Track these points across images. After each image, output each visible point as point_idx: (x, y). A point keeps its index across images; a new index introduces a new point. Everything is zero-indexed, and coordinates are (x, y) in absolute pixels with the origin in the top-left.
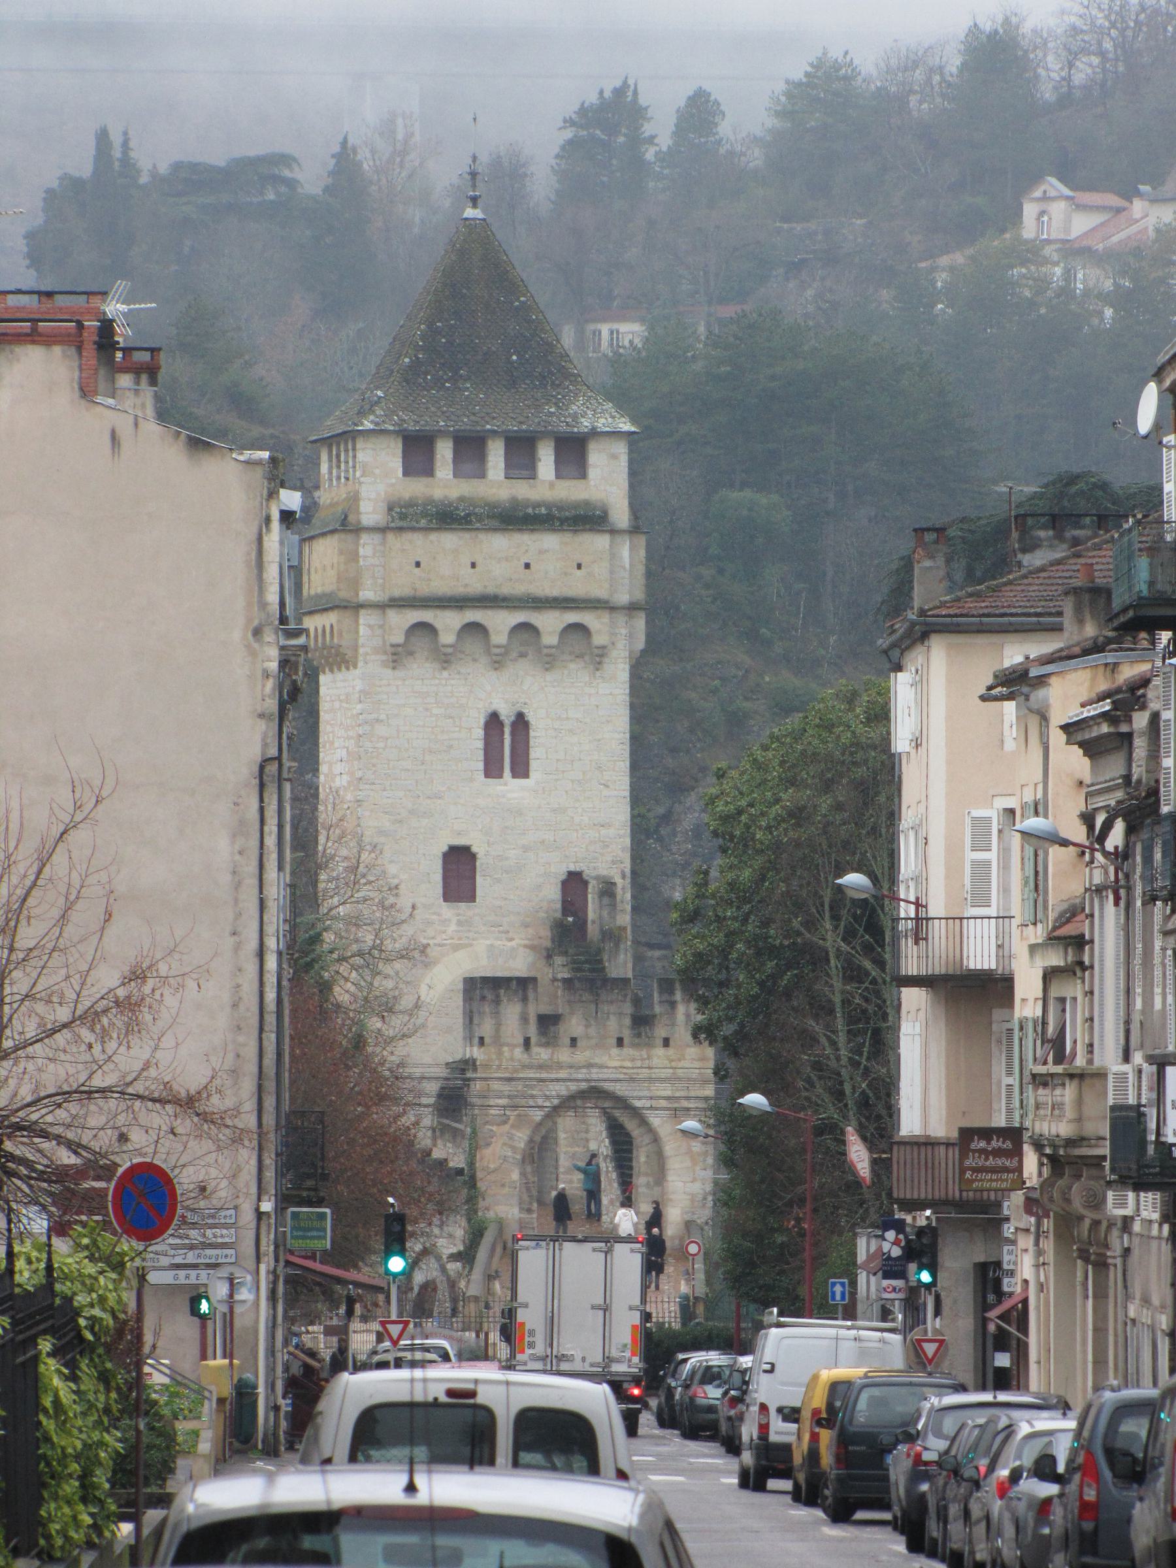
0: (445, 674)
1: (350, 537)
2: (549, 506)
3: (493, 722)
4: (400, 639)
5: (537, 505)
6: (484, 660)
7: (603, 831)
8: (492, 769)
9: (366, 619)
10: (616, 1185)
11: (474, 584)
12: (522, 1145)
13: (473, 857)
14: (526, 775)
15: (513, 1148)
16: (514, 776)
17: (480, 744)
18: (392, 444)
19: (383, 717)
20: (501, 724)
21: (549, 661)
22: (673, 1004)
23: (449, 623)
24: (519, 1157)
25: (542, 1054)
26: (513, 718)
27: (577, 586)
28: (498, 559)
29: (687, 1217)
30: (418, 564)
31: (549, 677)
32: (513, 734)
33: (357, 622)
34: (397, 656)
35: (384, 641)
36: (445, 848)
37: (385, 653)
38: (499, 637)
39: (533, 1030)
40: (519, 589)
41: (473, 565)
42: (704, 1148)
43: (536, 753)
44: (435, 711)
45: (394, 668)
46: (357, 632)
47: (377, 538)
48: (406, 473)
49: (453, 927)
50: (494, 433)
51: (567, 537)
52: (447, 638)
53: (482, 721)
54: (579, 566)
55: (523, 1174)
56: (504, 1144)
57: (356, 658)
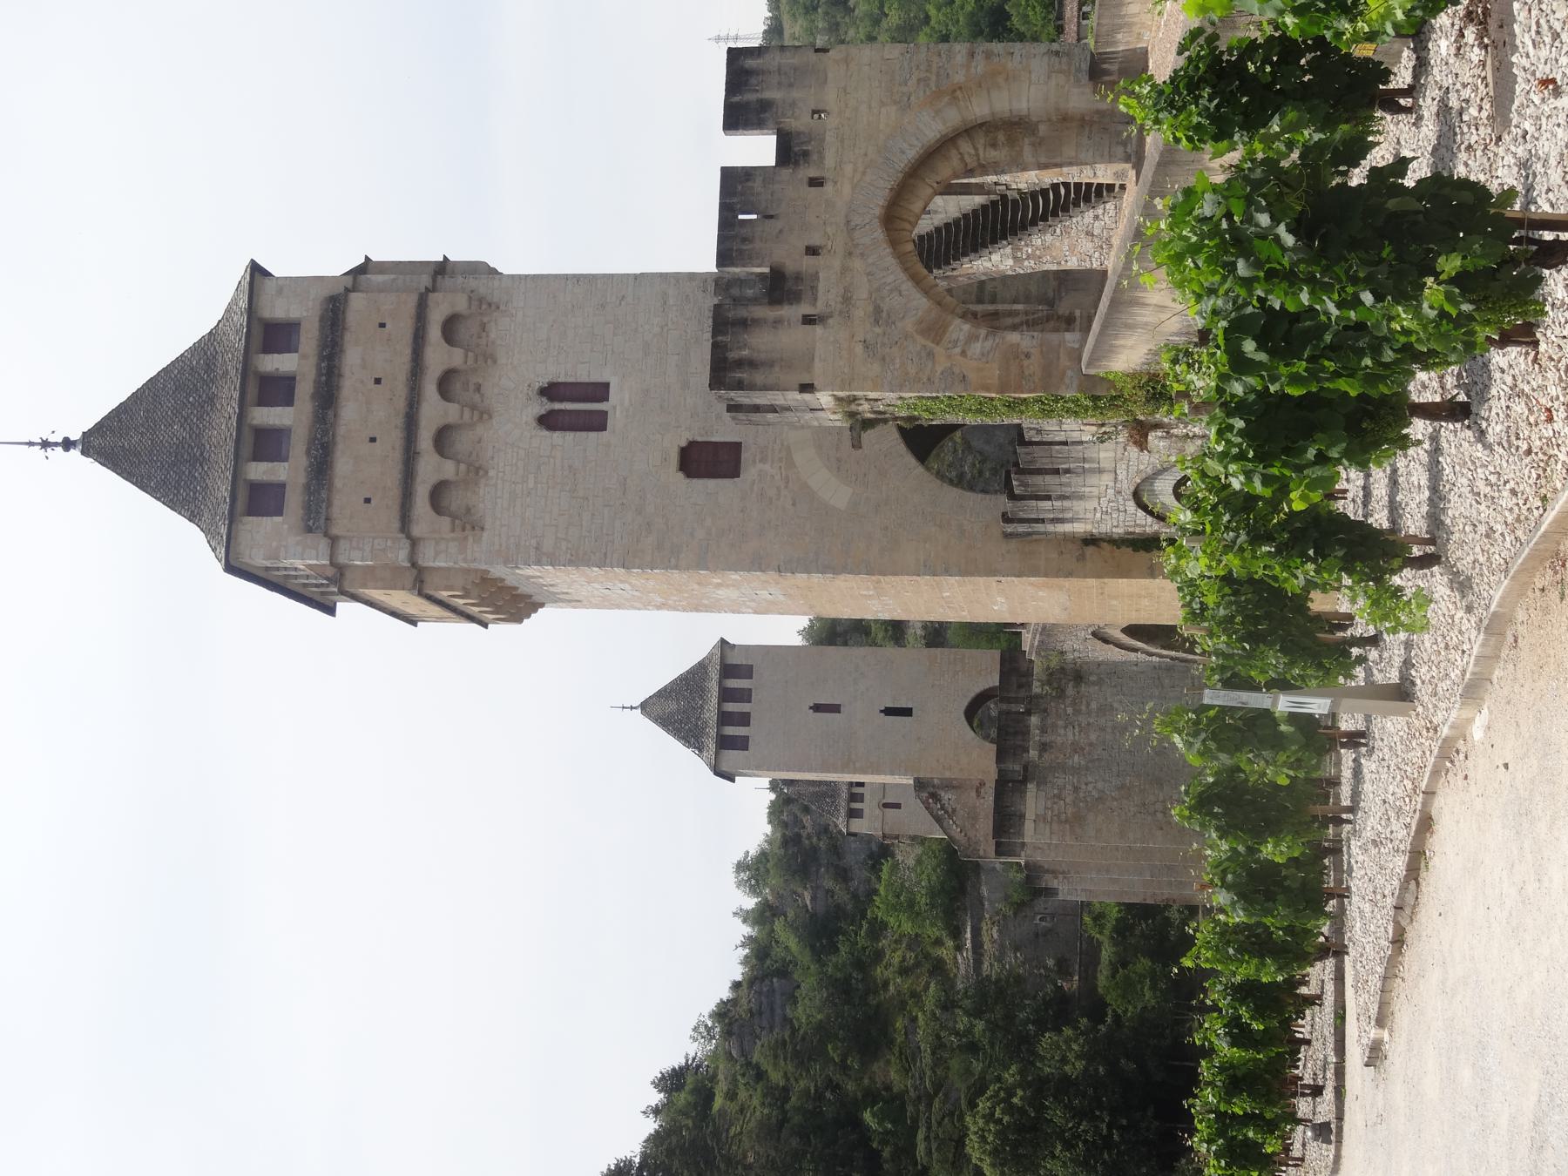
0: (492, 473)
1: (348, 575)
2: (321, 358)
3: (548, 422)
4: (445, 522)
5: (319, 374)
6: (480, 430)
7: (671, 302)
8: (598, 423)
9: (428, 558)
10: (1048, 238)
11: (393, 439)
12: (967, 327)
13: (692, 444)
14: (606, 385)
15: (972, 338)
16: (607, 399)
17: (570, 436)
18: (248, 527)
19: (533, 542)
20: (551, 412)
21: (488, 358)
22: (765, 105)
23: (430, 468)
24: (983, 332)
25: (827, 295)
26: (544, 399)
27: (403, 328)
28: (366, 412)
29: (1085, 78)
30: (368, 501)
31: (502, 360)
32: (561, 401)
33: (440, 568)
34: (468, 523)
35: (453, 539)
36: (681, 475)
37: (466, 538)
38: (451, 413)
39: (793, 312)
40: (401, 390)
41: (373, 440)
42: (979, 57)
43: (585, 374)
44: (531, 485)
45: (483, 529)
46: (449, 569)
47: (343, 545)
48: (281, 514)
49: (767, 467)
50: (241, 416)
51: (348, 337)
52: (449, 469)
53: (546, 433)
54: (382, 325)
55: (1014, 328)
56: (963, 353)
57: (476, 571)
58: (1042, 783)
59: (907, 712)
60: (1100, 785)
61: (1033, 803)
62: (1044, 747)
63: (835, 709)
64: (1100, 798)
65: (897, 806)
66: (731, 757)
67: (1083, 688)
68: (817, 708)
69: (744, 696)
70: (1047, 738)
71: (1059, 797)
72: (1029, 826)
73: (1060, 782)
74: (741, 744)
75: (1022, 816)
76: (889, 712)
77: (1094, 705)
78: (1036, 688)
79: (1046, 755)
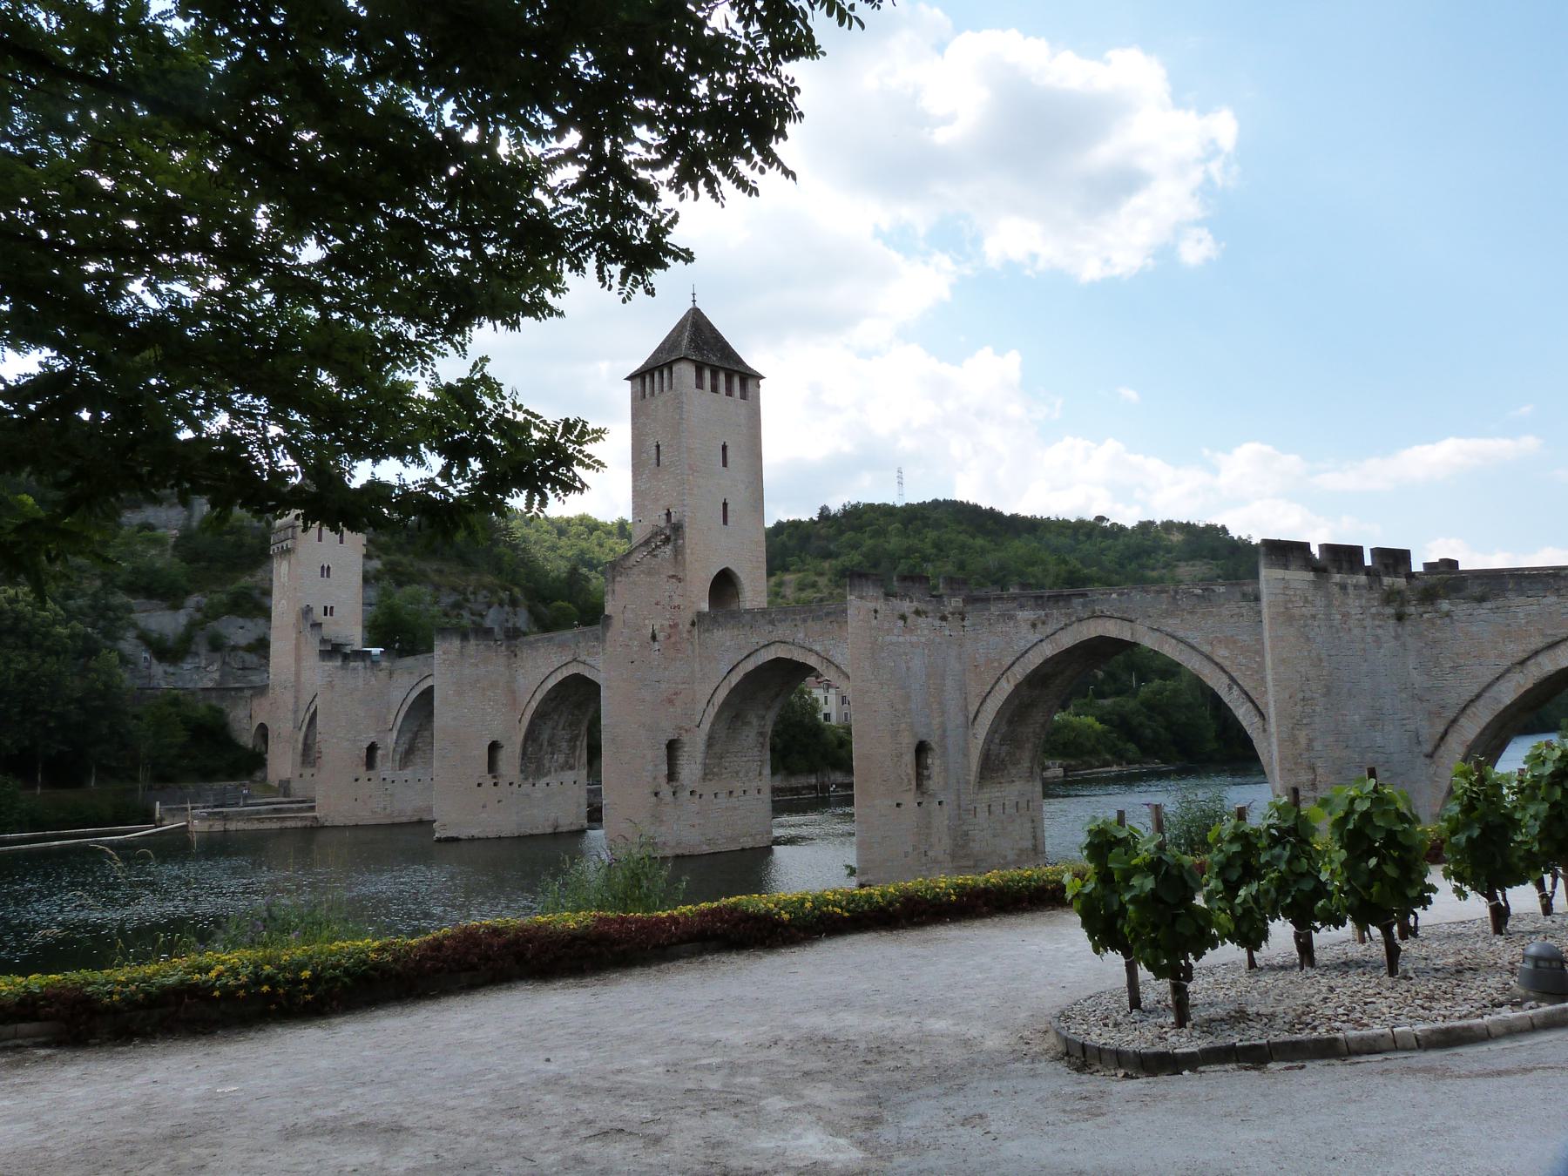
58: (1316, 585)
59: (725, 522)
60: (1319, 639)
61: (1299, 578)
62: (1343, 587)
63: (725, 464)
64: (1308, 639)
65: (320, 539)
66: (686, 372)
67: (1392, 622)
68: (724, 448)
69: (729, 392)
70: (1350, 590)
71: (1306, 601)
72: (1279, 573)
73: (1318, 603)
74: (700, 386)
75: (1286, 567)
76: (725, 505)
77: (1380, 631)
78: (1387, 581)
79: (1336, 589)
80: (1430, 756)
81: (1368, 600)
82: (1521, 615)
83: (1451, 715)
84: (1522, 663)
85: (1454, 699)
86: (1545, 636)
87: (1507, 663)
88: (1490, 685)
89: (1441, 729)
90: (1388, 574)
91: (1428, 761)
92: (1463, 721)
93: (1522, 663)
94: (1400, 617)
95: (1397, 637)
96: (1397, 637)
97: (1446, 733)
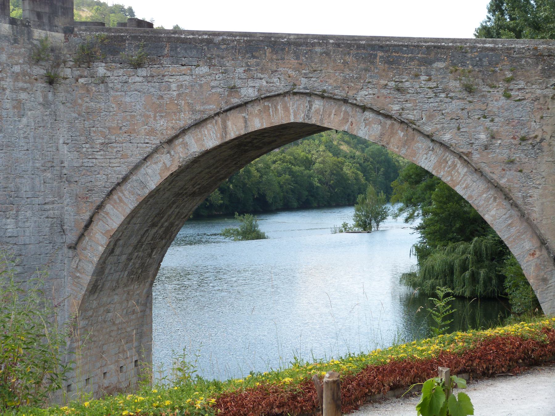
67: (41, 85)
77: (23, 96)
78: (38, 34)
80: (73, 247)
81: (11, 56)
82: (174, 86)
83: (97, 199)
84: (170, 141)
85: (102, 182)
86: (194, 111)
87: (156, 141)
88: (137, 167)
89: (86, 216)
90: (41, 26)
91: (71, 253)
92: (108, 207)
93: (170, 141)
94: (51, 81)
95: (46, 104)
96: (46, 104)
97: (90, 221)
